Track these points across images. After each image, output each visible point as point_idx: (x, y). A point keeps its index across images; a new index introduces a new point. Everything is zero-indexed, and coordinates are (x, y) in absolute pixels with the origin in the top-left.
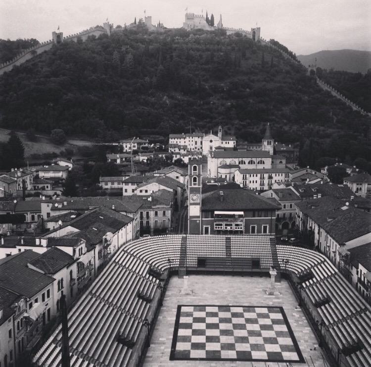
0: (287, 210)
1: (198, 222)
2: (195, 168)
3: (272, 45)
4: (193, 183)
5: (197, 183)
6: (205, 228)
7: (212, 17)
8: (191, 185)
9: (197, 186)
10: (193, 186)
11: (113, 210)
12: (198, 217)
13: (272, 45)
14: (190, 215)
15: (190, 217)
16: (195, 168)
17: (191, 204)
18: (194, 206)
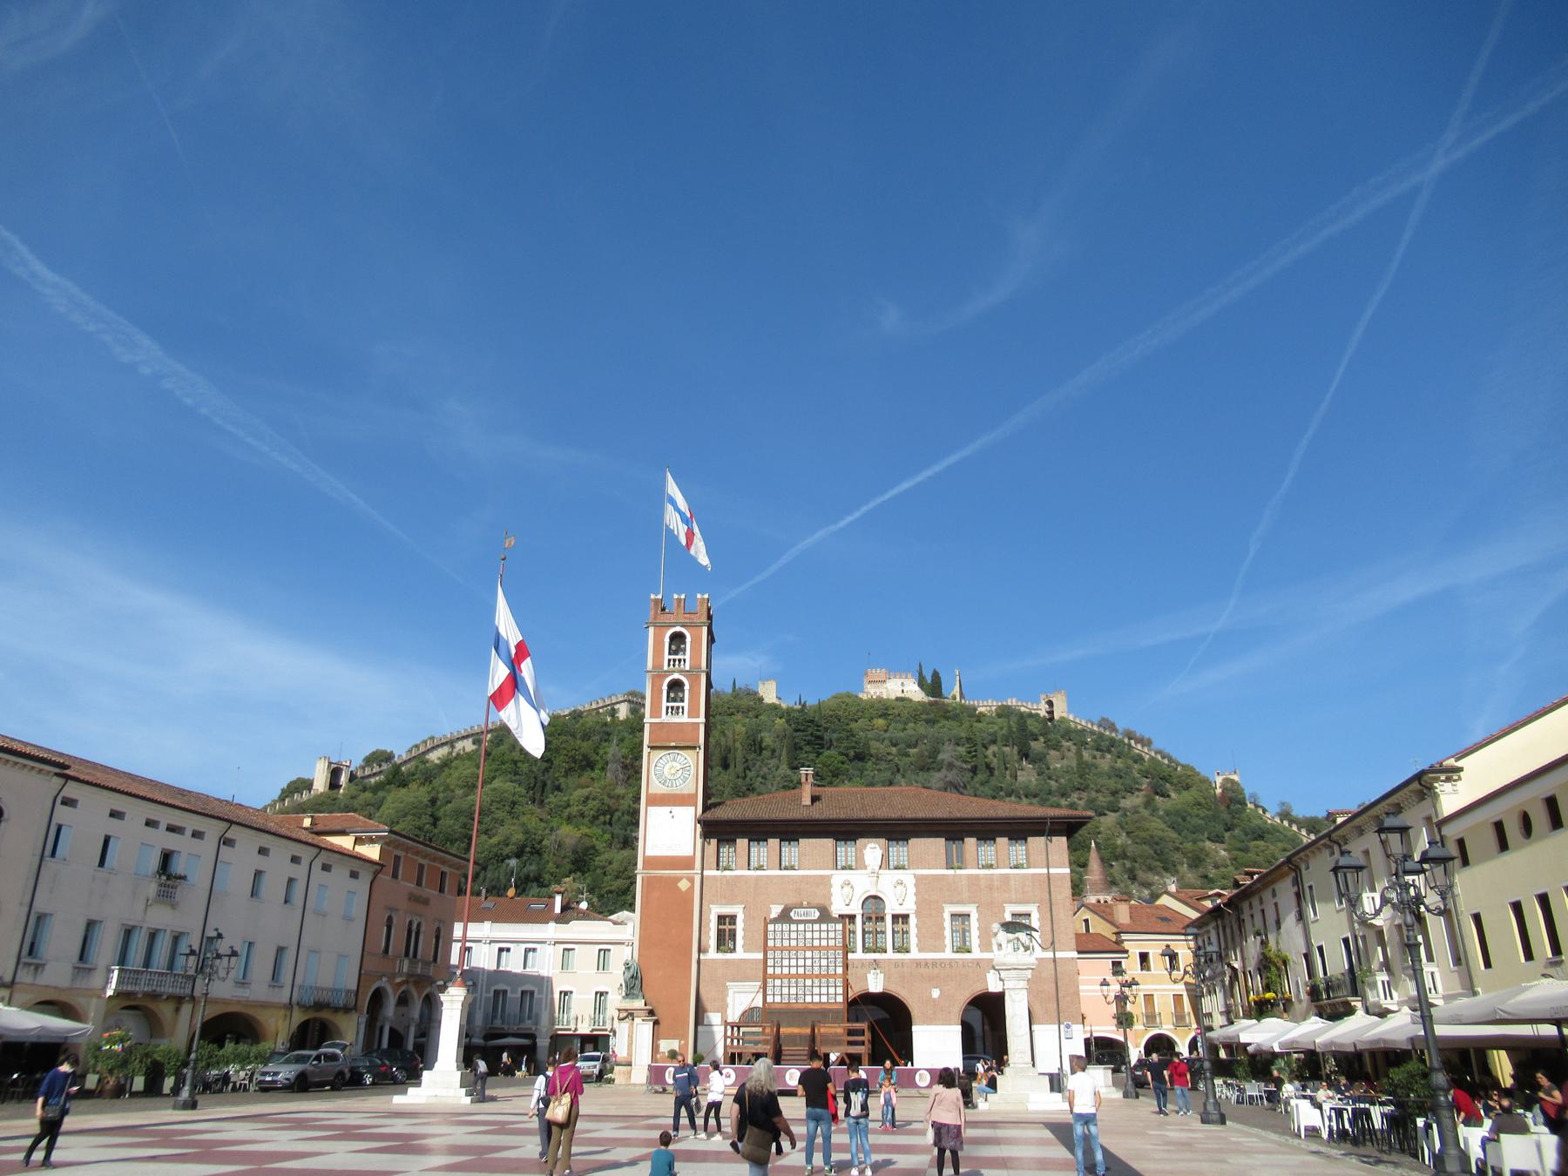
0: (1157, 980)
1: (683, 885)
2: (678, 639)
3: (1102, 730)
4: (665, 704)
5: (686, 704)
6: (721, 919)
7: (936, 676)
8: (656, 712)
9: (684, 719)
10: (665, 718)
11: (306, 829)
12: (686, 863)
13: (1102, 730)
14: (649, 853)
15: (653, 862)
16: (678, 639)
17: (658, 800)
18: (665, 810)
